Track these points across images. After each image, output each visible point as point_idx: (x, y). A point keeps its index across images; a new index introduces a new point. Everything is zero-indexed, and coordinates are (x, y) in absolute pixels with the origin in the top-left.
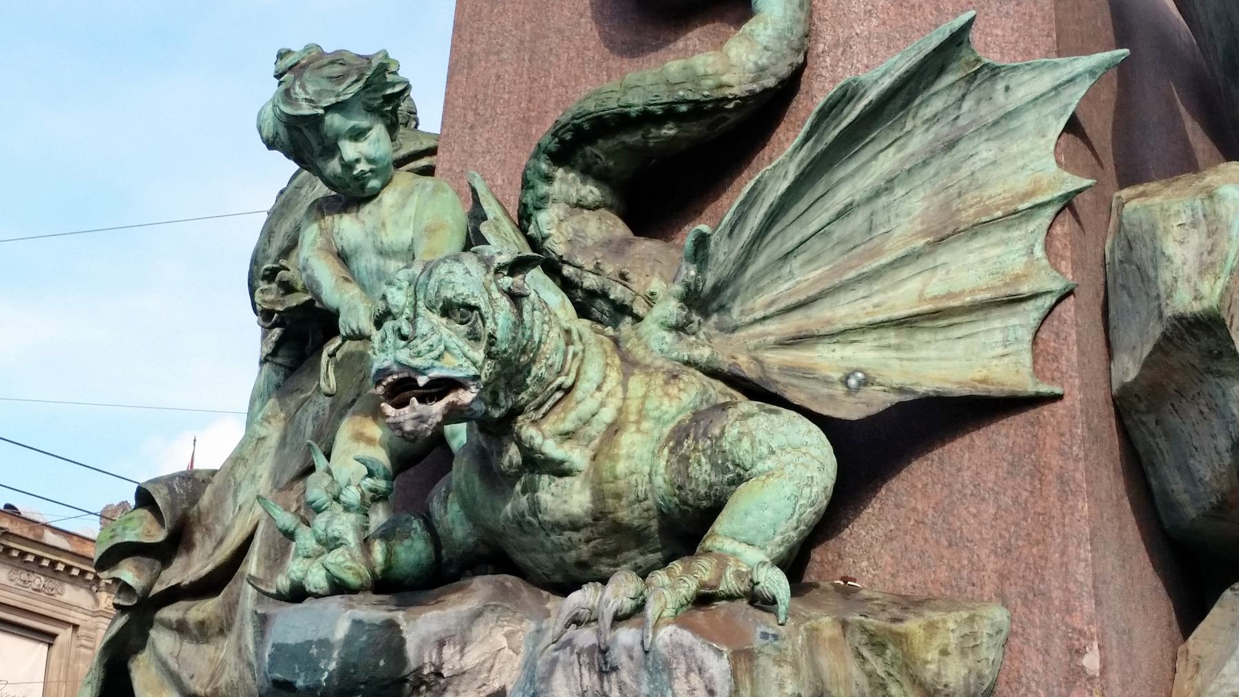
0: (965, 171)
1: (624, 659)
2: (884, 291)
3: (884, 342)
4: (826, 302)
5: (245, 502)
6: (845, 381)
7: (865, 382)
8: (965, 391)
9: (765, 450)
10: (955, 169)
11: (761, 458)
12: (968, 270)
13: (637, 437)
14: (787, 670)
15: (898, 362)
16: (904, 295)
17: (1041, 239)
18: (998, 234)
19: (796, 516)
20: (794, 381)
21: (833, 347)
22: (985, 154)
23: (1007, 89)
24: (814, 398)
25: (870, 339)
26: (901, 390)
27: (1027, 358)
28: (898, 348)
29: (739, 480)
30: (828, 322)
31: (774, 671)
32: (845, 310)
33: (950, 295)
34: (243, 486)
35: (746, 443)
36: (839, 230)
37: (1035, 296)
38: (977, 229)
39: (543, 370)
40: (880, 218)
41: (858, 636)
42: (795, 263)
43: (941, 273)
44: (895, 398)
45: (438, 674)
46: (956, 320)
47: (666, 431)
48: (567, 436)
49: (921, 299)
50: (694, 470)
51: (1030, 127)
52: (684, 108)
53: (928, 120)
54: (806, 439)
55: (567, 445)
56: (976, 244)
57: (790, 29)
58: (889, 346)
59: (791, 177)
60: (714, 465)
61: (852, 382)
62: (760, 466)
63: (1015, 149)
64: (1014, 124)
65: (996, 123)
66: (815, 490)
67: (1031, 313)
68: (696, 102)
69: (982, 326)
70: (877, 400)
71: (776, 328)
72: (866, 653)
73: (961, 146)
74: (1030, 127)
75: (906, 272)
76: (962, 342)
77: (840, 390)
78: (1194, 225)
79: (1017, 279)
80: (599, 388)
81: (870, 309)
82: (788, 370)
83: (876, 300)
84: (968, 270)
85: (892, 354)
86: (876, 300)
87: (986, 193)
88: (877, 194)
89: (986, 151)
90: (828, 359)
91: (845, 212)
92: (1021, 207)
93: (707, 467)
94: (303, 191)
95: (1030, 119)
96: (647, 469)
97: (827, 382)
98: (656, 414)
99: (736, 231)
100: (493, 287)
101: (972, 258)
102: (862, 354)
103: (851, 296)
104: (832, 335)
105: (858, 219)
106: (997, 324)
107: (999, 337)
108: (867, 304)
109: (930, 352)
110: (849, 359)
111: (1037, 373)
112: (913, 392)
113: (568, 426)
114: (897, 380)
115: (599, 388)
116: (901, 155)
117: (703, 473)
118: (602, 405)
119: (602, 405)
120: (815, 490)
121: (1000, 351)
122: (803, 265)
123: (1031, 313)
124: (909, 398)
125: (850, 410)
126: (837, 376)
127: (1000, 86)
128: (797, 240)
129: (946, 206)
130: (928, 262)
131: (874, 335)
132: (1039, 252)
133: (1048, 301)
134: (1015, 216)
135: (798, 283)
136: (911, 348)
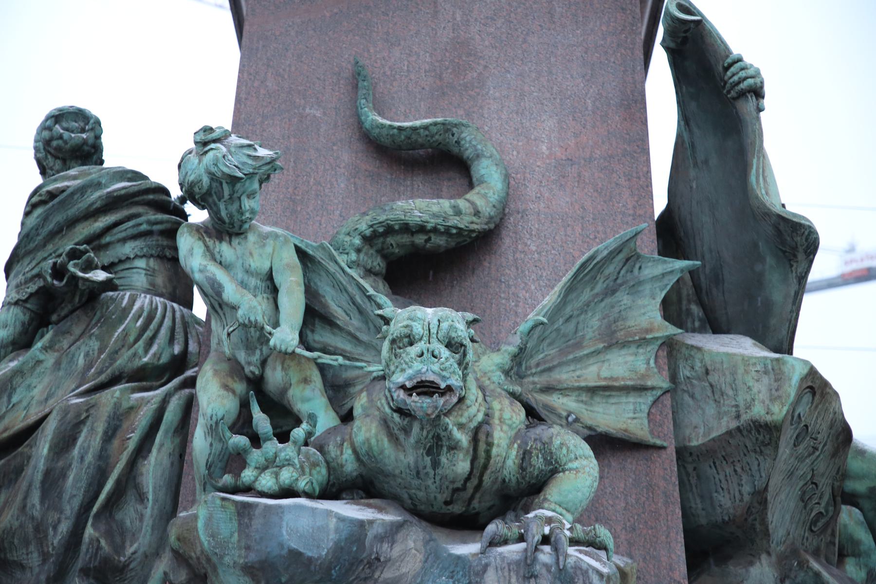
0: (616, 309)
1: (544, 571)
3: (580, 399)
5: (20, 402)
9: (573, 456)
11: (571, 461)
12: (621, 365)
16: (592, 373)
17: (653, 357)
18: (633, 349)
22: (625, 302)
23: (640, 268)
27: (646, 422)
28: (585, 403)
30: (559, 382)
32: (565, 376)
33: (612, 378)
34: (18, 390)
35: (564, 451)
37: (653, 388)
38: (625, 345)
40: (580, 327)
43: (606, 364)
45: (378, 559)
46: (613, 393)
50: (534, 461)
51: (647, 292)
52: (454, 231)
56: (624, 352)
58: (582, 401)
60: (545, 459)
61: (570, 419)
62: (570, 465)
63: (640, 302)
64: (640, 288)
65: (633, 285)
67: (649, 398)
68: (461, 229)
69: (624, 399)
74: (647, 292)
75: (592, 361)
76: (614, 406)
78: (766, 372)
79: (643, 377)
83: (578, 373)
93: (541, 460)
94: (76, 197)
101: (620, 360)
104: (561, 390)
106: (631, 399)
107: (631, 407)
111: (651, 432)
112: (595, 430)
114: (589, 423)
116: (592, 293)
117: (538, 463)
121: (631, 415)
123: (649, 398)
124: (593, 433)
126: (564, 414)
129: (609, 326)
130: (601, 357)
131: (577, 393)
132: (652, 362)
133: (659, 393)
134: (643, 342)
135: (546, 355)
136: (591, 405)
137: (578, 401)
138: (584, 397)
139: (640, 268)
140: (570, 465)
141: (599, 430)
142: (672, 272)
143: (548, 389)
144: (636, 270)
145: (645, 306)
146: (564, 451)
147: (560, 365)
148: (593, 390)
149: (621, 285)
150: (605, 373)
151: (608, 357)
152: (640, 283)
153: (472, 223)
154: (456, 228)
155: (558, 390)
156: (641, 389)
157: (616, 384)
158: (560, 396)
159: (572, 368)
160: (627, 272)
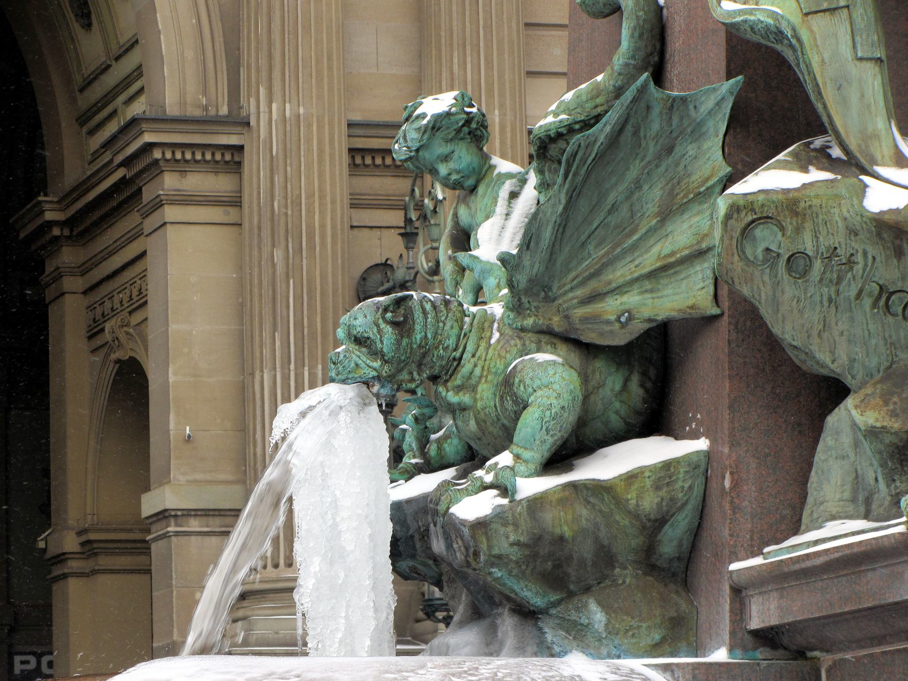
2: (641, 255)
3: (644, 289)
4: (610, 269)
6: (618, 320)
7: (630, 319)
8: (681, 316)
9: (530, 390)
10: (677, 164)
11: (530, 395)
12: (681, 235)
13: (485, 386)
14: (510, 528)
15: (651, 300)
18: (696, 208)
19: (544, 428)
20: (590, 326)
21: (616, 297)
22: (690, 153)
23: (695, 107)
24: (602, 334)
25: (636, 289)
26: (650, 320)
28: (651, 291)
29: (524, 408)
30: (610, 283)
31: (502, 530)
32: (621, 273)
33: (673, 253)
35: (522, 388)
36: (613, 220)
38: (683, 208)
39: (441, 351)
41: (585, 492)
42: (591, 247)
43: (670, 237)
44: (647, 326)
46: (678, 269)
47: (501, 378)
48: (459, 389)
49: (659, 258)
53: (653, 139)
54: (552, 380)
55: (461, 394)
56: (686, 216)
57: (633, 57)
59: (563, 201)
61: (623, 319)
64: (704, 129)
66: (553, 411)
68: (583, 121)
70: (638, 327)
71: (580, 292)
72: (592, 500)
73: (677, 149)
76: (684, 282)
77: (617, 325)
80: (473, 356)
81: (633, 269)
82: (585, 320)
83: (637, 262)
84: (681, 235)
85: (648, 296)
86: (637, 262)
87: (694, 178)
88: (632, 194)
89: (691, 150)
90: (611, 306)
91: (614, 208)
92: (702, 189)
95: (710, 124)
96: (492, 404)
97: (608, 322)
98: (494, 370)
99: (532, 244)
100: (381, 321)
101: (685, 226)
102: (631, 299)
103: (623, 263)
104: (612, 291)
105: (624, 211)
106: (698, 268)
107: (700, 276)
108: (632, 266)
109: (669, 291)
110: (625, 303)
112: (655, 320)
113: (458, 382)
115: (473, 356)
118: (475, 366)
119: (475, 366)
120: (553, 411)
121: (701, 285)
122: (596, 247)
124: (654, 324)
125: (621, 339)
126: (613, 318)
127: (691, 107)
128: (587, 234)
129: (672, 189)
130: (663, 232)
131: (636, 286)
136: (658, 290)
137: (642, 293)
138: (647, 285)
139: (695, 107)
140: (532, 399)
141: (660, 318)
142: (723, 99)
143: (595, 297)
144: (692, 112)
145: (710, 148)
146: (522, 388)
147: (618, 258)
148: (652, 275)
149: (676, 138)
150: (666, 251)
151: (669, 230)
152: (701, 124)
153: (596, 107)
154: (576, 123)
155: (607, 293)
156: (699, 254)
157: (672, 260)
158: (617, 297)
159: (629, 259)
160: (681, 119)
